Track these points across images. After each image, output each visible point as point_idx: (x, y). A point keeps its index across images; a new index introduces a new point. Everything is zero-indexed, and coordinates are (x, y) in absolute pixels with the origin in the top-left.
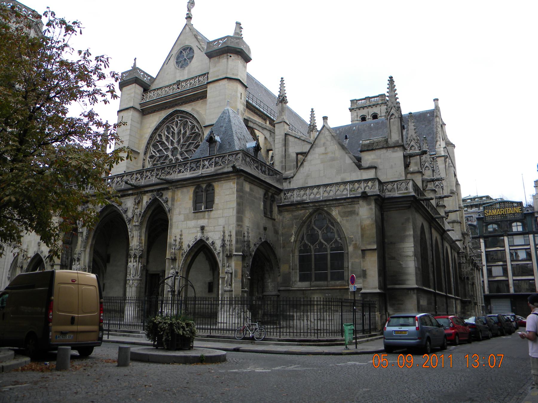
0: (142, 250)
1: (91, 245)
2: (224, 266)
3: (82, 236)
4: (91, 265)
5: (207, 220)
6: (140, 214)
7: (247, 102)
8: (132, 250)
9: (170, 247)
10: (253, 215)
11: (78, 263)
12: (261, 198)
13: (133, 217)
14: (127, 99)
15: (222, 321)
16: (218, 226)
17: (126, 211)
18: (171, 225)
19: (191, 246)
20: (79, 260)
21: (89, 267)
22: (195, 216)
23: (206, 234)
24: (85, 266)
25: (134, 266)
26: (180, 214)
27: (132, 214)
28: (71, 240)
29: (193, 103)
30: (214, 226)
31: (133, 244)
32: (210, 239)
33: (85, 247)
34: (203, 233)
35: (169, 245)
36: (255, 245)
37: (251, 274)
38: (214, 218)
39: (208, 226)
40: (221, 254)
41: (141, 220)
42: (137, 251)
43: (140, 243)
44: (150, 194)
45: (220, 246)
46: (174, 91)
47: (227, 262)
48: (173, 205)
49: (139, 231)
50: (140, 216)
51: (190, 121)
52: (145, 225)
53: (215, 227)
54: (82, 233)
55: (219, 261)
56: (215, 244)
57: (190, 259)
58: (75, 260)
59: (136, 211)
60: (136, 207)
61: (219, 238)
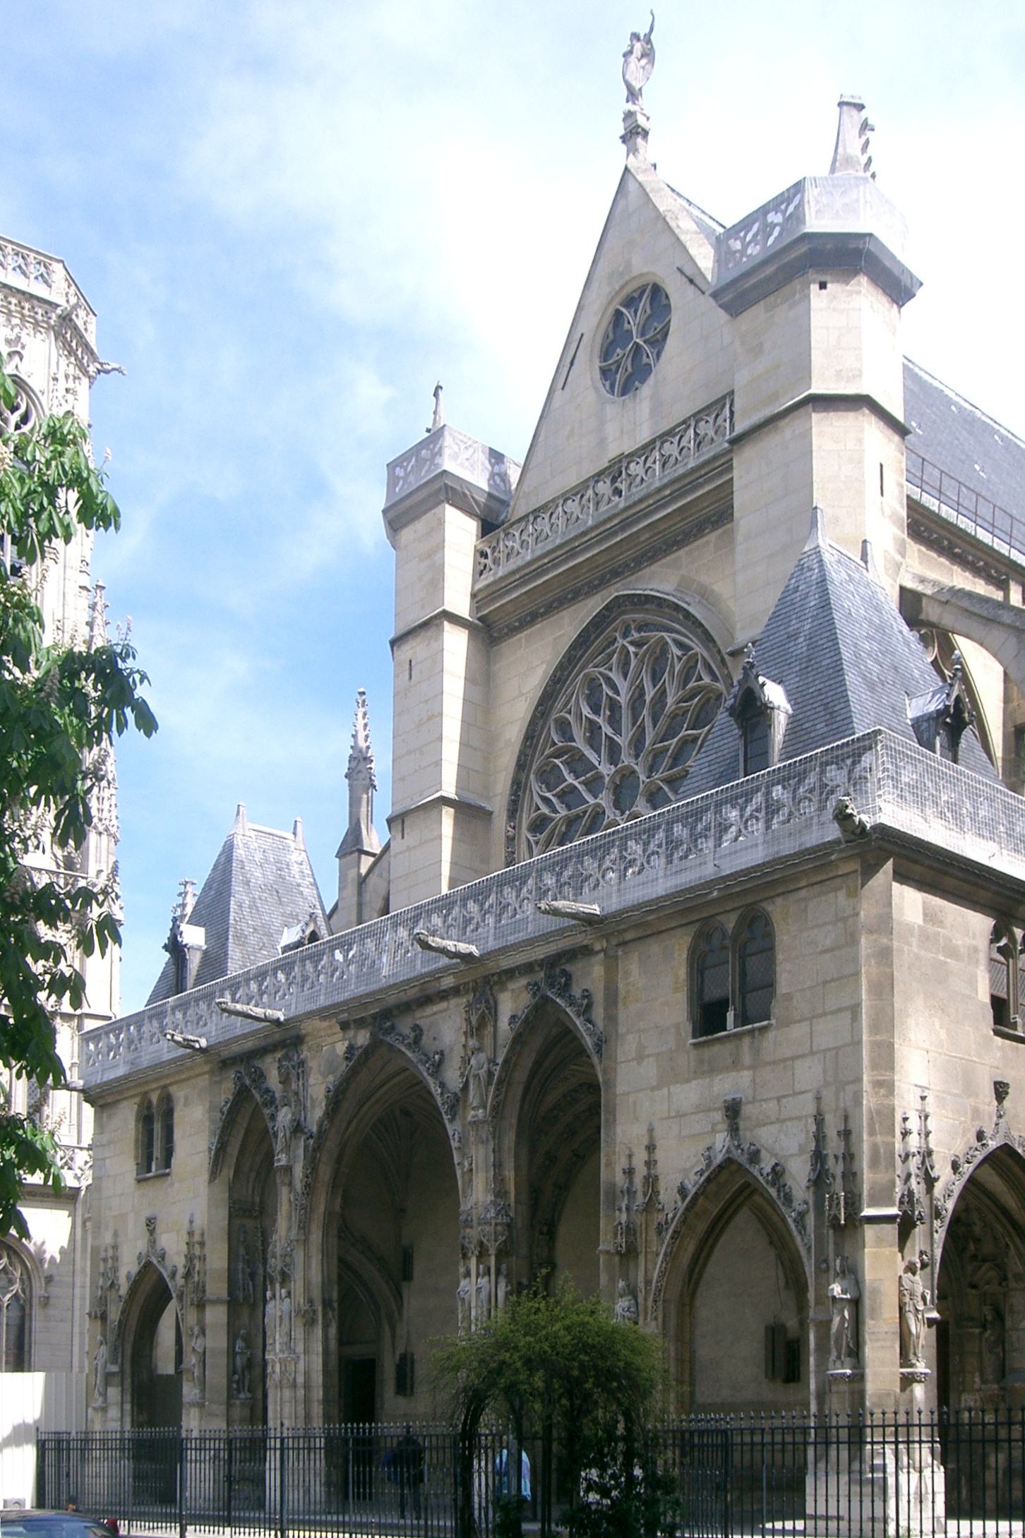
0: (509, 1225)
1: (329, 1214)
2: (828, 1269)
3: (290, 1184)
4: (335, 1295)
5: (747, 1075)
6: (490, 1074)
7: (913, 506)
8: (468, 1224)
9: (612, 1203)
10: (943, 1034)
11: (283, 1291)
12: (976, 950)
13: (465, 1088)
14: (420, 579)
15: (832, 1512)
16: (795, 1094)
17: (437, 1068)
18: (612, 1112)
19: (692, 1191)
20: (285, 1278)
21: (326, 1303)
22: (701, 1061)
23: (746, 1135)
24: (311, 1301)
25: (479, 1290)
26: (640, 1058)
27: (462, 1075)
28: (257, 1199)
29: (682, 552)
30: (779, 1099)
31: (473, 1199)
32: (763, 1153)
33: (304, 1227)
34: (734, 1130)
35: (606, 1193)
36: (955, 1166)
37: (943, 1297)
38: (774, 1063)
39: (754, 1101)
40: (810, 1220)
41: (496, 1096)
42: (487, 1228)
43: (500, 1193)
44: (523, 982)
45: (804, 1183)
46: (603, 508)
47: (837, 1255)
48: (611, 1019)
49: (491, 1146)
50: (489, 1083)
51: (676, 642)
52: (511, 1120)
53: (784, 1100)
54: (288, 1169)
55: (803, 1252)
56: (787, 1175)
57: (691, 1247)
58: (272, 1283)
59: (473, 1062)
60: (472, 1043)
61: (802, 1149)
